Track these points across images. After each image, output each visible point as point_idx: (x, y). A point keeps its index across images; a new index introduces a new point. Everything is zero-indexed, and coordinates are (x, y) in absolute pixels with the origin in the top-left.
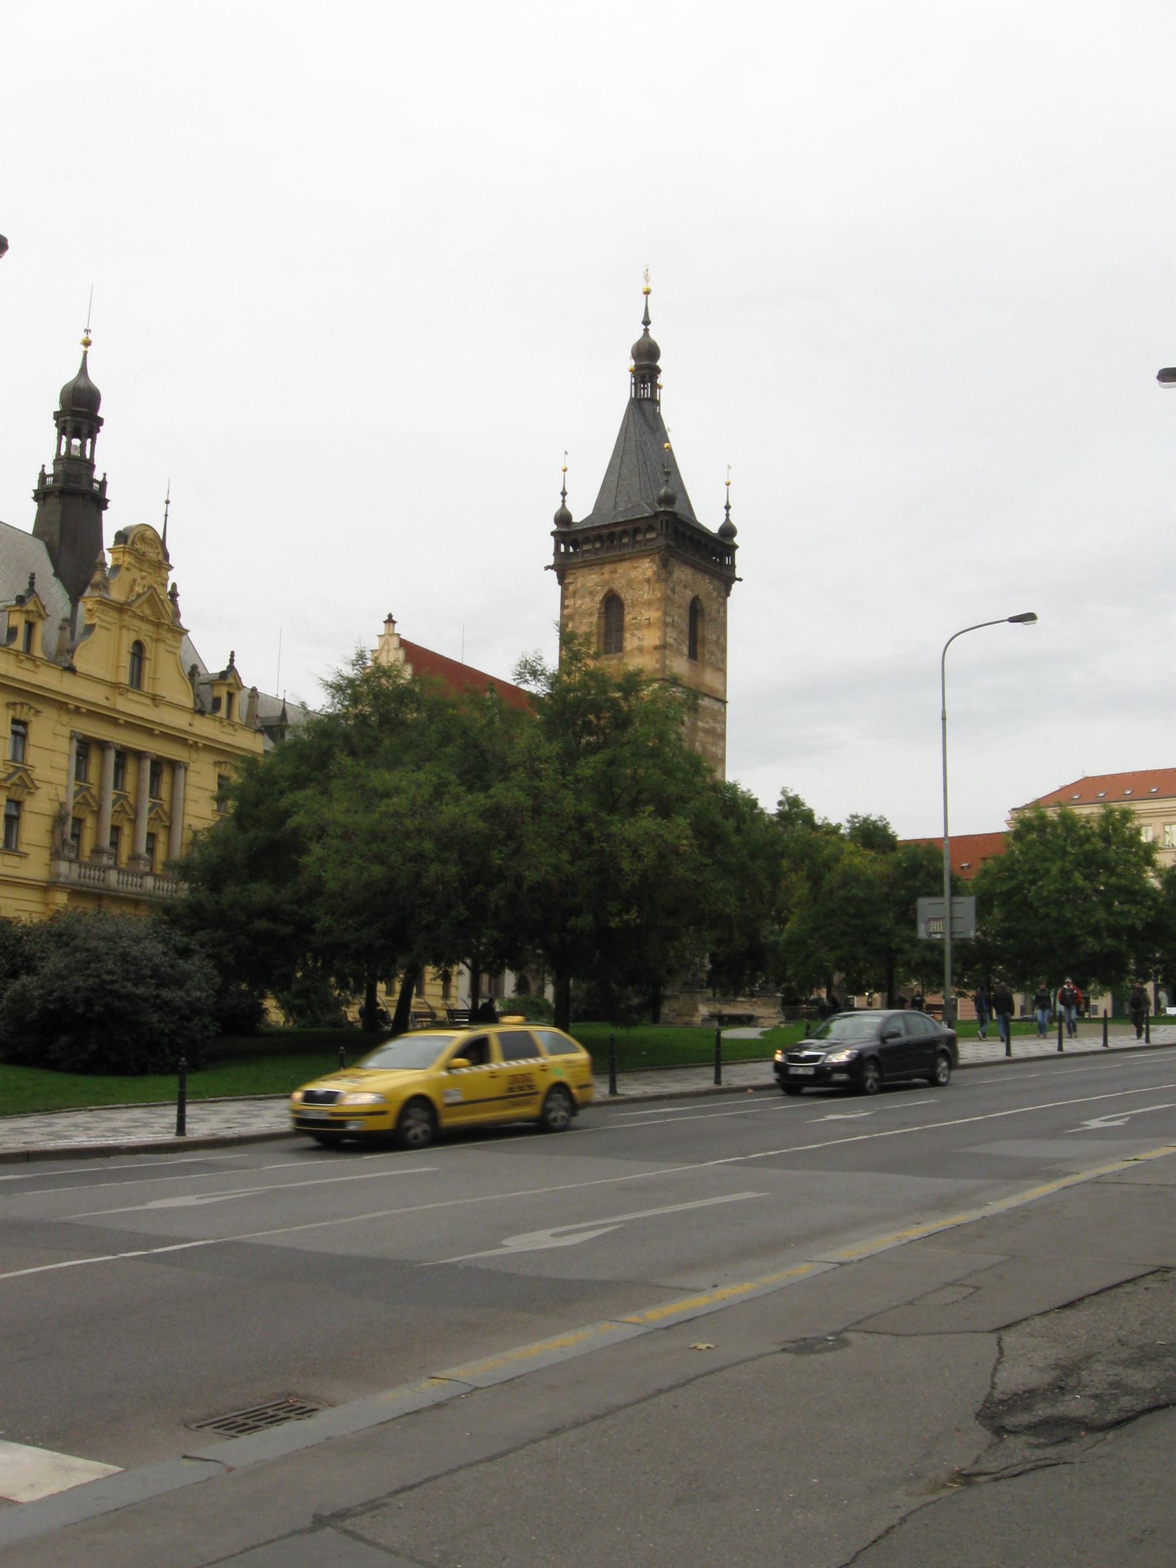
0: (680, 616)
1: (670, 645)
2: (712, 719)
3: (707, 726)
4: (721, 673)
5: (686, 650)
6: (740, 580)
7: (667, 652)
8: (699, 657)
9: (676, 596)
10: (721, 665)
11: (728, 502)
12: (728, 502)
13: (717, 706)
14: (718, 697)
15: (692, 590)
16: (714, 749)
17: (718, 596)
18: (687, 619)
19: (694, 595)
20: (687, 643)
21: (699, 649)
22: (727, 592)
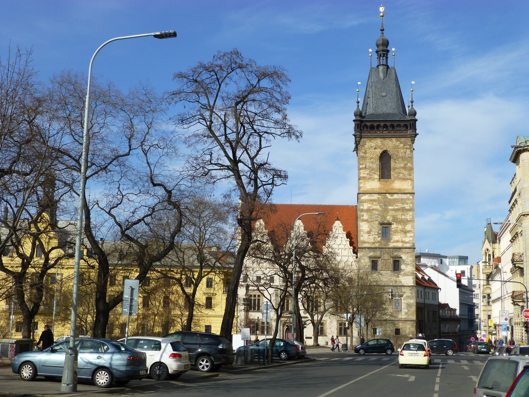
0: (372, 162)
1: (364, 178)
2: (401, 203)
3: (396, 208)
4: (410, 181)
5: (377, 177)
6: (418, 134)
7: (361, 181)
8: (392, 177)
9: (367, 155)
10: (408, 177)
11: (412, 99)
12: (412, 99)
13: (404, 196)
14: (406, 192)
15: (381, 149)
16: (403, 217)
17: (404, 145)
18: (378, 162)
19: (381, 151)
20: (378, 173)
21: (392, 173)
22: (413, 141)
